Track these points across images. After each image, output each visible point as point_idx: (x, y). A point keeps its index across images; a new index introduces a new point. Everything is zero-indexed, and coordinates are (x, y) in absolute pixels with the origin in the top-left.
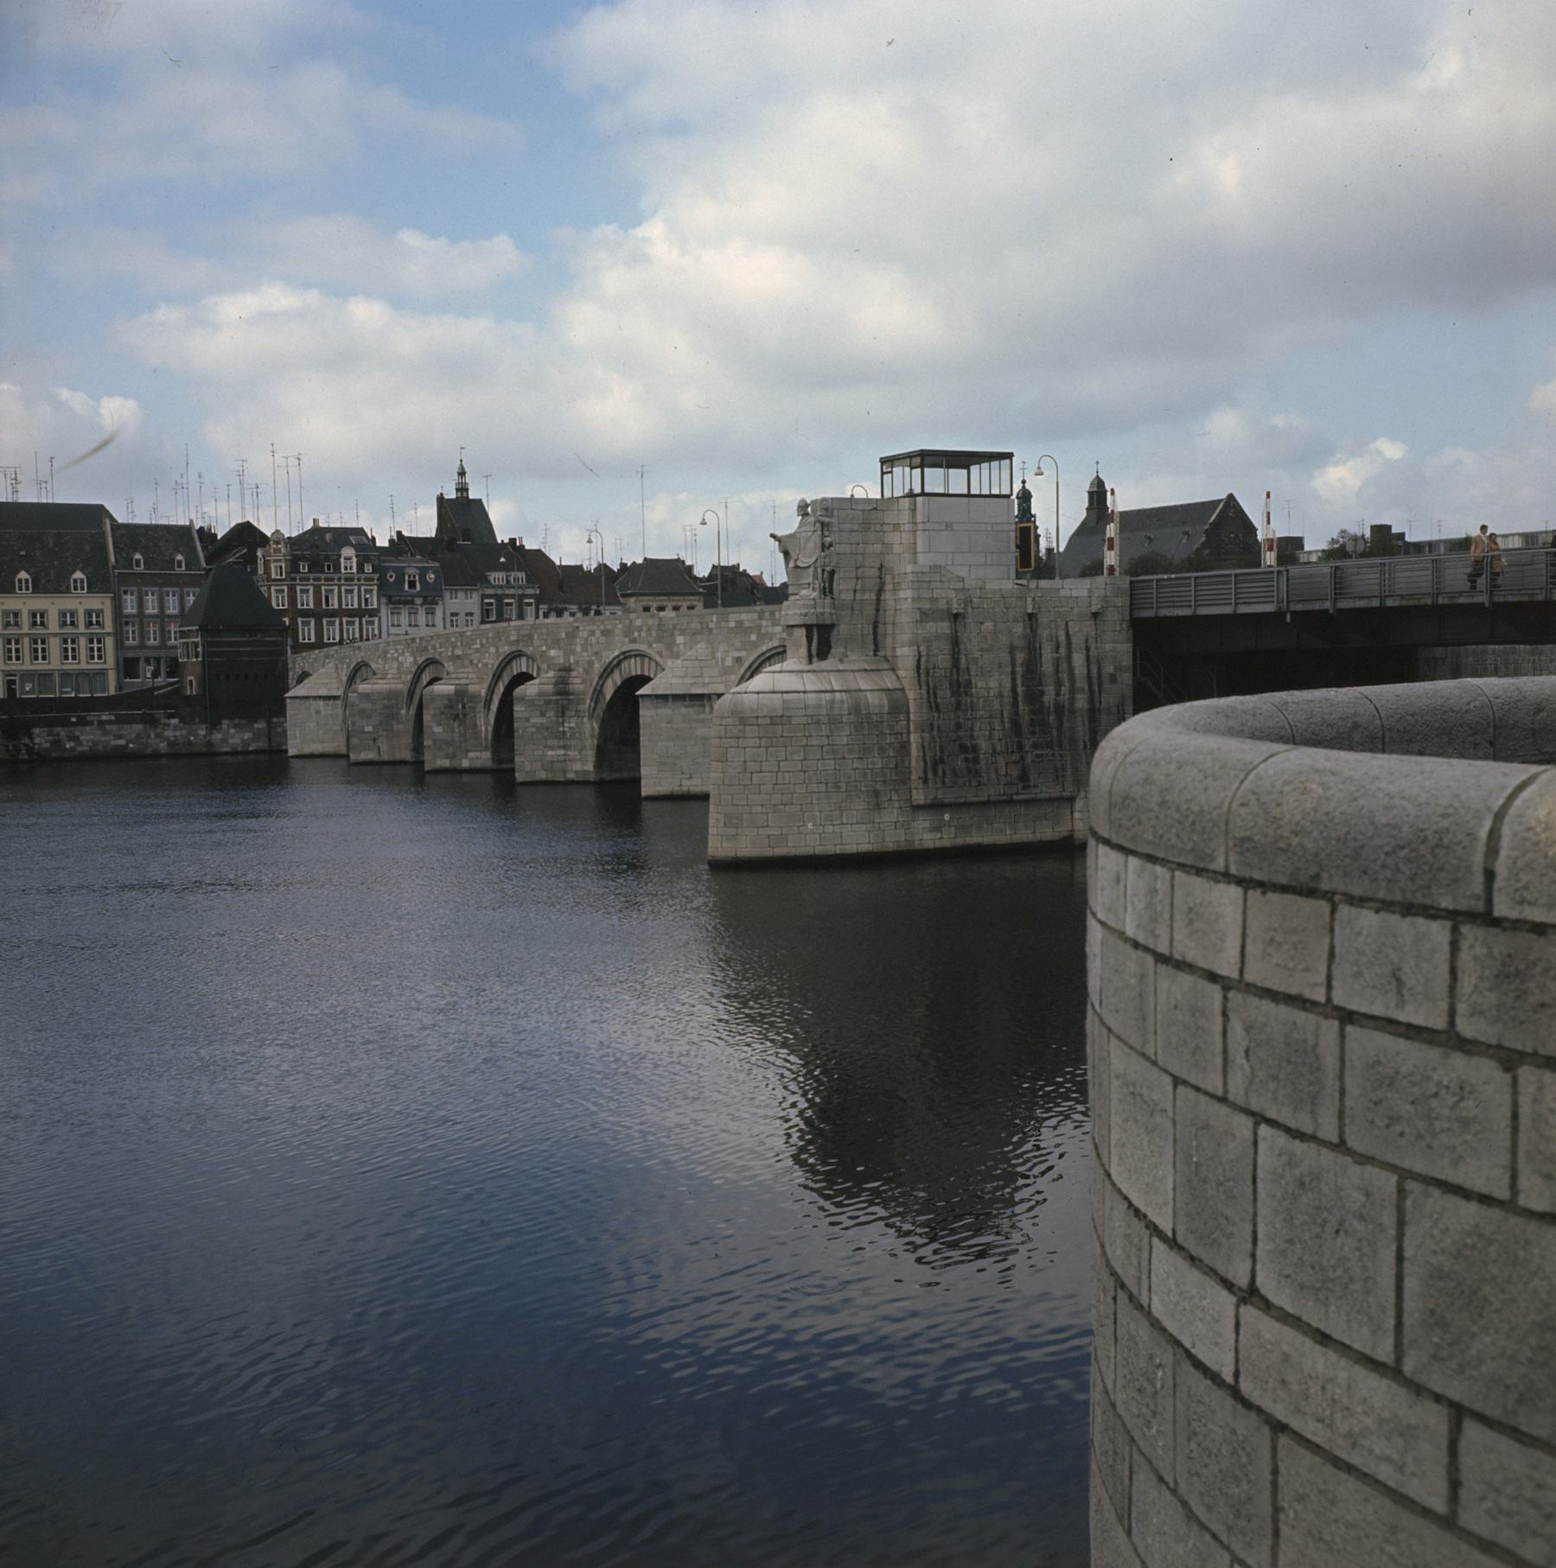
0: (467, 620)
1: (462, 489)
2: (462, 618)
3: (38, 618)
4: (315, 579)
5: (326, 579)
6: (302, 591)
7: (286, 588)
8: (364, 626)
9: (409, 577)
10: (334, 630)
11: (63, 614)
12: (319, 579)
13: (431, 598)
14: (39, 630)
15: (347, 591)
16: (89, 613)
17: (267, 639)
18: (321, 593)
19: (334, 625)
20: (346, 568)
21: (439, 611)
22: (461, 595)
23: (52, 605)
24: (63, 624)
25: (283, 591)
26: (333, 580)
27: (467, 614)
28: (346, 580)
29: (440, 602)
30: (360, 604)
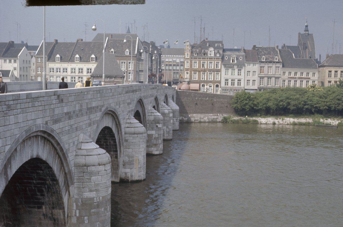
0: (253, 74)
1: (307, 30)
2: (251, 73)
3: (81, 70)
4: (199, 58)
5: (203, 59)
6: (194, 62)
7: (189, 61)
8: (215, 75)
9: (233, 58)
10: (196, 75)
11: (72, 69)
12: (200, 58)
13: (240, 66)
14: (81, 74)
15: (210, 63)
16: (57, 69)
17: (116, 80)
18: (201, 63)
19: (205, 74)
20: (210, 54)
21: (243, 71)
22: (251, 65)
23: (85, 66)
24: (72, 72)
25: (188, 62)
26: (205, 59)
27: (253, 72)
28: (210, 59)
29: (244, 67)
30: (214, 67)
